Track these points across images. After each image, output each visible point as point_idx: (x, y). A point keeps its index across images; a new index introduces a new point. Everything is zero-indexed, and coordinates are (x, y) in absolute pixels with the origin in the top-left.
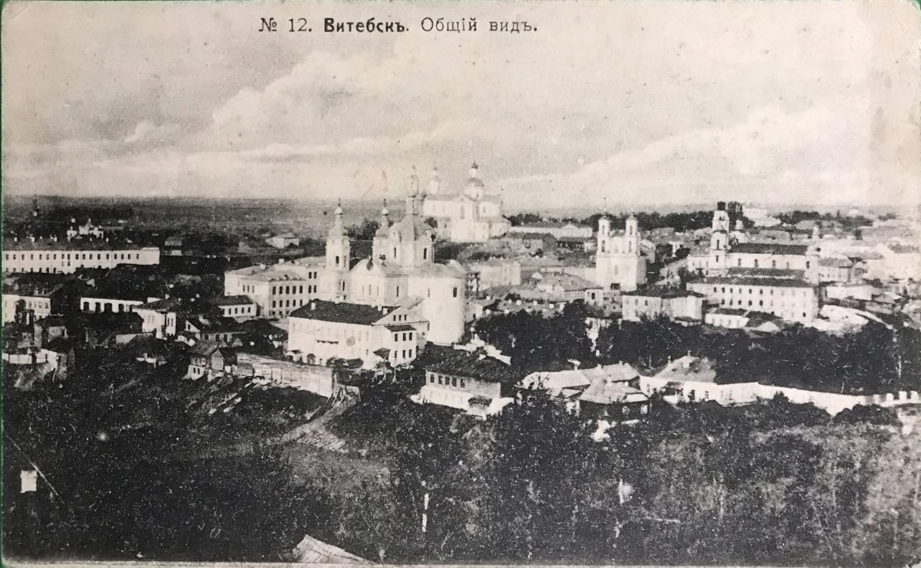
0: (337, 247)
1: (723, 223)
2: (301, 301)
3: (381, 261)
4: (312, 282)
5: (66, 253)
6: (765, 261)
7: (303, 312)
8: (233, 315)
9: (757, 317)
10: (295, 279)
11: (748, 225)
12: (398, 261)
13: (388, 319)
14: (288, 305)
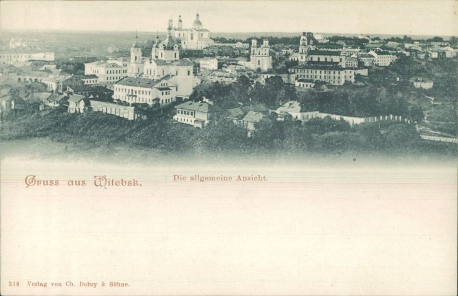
0: (135, 53)
1: (305, 42)
2: (120, 77)
3: (155, 59)
4: (125, 68)
5: (9, 55)
6: (322, 58)
7: (120, 81)
8: (89, 83)
9: (318, 84)
10: (117, 67)
11: (316, 42)
12: (163, 59)
13: (158, 85)
14: (114, 79)
